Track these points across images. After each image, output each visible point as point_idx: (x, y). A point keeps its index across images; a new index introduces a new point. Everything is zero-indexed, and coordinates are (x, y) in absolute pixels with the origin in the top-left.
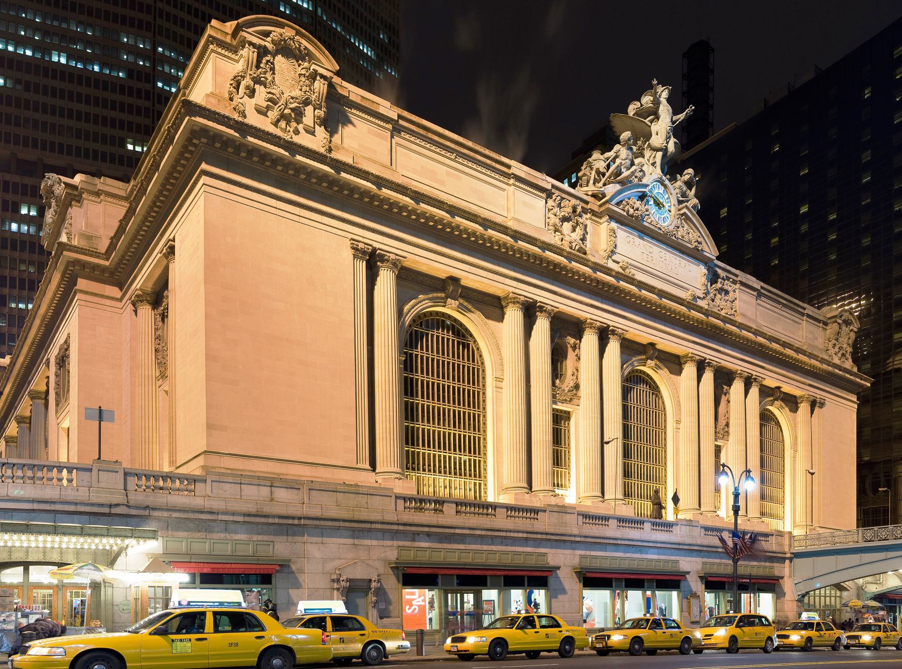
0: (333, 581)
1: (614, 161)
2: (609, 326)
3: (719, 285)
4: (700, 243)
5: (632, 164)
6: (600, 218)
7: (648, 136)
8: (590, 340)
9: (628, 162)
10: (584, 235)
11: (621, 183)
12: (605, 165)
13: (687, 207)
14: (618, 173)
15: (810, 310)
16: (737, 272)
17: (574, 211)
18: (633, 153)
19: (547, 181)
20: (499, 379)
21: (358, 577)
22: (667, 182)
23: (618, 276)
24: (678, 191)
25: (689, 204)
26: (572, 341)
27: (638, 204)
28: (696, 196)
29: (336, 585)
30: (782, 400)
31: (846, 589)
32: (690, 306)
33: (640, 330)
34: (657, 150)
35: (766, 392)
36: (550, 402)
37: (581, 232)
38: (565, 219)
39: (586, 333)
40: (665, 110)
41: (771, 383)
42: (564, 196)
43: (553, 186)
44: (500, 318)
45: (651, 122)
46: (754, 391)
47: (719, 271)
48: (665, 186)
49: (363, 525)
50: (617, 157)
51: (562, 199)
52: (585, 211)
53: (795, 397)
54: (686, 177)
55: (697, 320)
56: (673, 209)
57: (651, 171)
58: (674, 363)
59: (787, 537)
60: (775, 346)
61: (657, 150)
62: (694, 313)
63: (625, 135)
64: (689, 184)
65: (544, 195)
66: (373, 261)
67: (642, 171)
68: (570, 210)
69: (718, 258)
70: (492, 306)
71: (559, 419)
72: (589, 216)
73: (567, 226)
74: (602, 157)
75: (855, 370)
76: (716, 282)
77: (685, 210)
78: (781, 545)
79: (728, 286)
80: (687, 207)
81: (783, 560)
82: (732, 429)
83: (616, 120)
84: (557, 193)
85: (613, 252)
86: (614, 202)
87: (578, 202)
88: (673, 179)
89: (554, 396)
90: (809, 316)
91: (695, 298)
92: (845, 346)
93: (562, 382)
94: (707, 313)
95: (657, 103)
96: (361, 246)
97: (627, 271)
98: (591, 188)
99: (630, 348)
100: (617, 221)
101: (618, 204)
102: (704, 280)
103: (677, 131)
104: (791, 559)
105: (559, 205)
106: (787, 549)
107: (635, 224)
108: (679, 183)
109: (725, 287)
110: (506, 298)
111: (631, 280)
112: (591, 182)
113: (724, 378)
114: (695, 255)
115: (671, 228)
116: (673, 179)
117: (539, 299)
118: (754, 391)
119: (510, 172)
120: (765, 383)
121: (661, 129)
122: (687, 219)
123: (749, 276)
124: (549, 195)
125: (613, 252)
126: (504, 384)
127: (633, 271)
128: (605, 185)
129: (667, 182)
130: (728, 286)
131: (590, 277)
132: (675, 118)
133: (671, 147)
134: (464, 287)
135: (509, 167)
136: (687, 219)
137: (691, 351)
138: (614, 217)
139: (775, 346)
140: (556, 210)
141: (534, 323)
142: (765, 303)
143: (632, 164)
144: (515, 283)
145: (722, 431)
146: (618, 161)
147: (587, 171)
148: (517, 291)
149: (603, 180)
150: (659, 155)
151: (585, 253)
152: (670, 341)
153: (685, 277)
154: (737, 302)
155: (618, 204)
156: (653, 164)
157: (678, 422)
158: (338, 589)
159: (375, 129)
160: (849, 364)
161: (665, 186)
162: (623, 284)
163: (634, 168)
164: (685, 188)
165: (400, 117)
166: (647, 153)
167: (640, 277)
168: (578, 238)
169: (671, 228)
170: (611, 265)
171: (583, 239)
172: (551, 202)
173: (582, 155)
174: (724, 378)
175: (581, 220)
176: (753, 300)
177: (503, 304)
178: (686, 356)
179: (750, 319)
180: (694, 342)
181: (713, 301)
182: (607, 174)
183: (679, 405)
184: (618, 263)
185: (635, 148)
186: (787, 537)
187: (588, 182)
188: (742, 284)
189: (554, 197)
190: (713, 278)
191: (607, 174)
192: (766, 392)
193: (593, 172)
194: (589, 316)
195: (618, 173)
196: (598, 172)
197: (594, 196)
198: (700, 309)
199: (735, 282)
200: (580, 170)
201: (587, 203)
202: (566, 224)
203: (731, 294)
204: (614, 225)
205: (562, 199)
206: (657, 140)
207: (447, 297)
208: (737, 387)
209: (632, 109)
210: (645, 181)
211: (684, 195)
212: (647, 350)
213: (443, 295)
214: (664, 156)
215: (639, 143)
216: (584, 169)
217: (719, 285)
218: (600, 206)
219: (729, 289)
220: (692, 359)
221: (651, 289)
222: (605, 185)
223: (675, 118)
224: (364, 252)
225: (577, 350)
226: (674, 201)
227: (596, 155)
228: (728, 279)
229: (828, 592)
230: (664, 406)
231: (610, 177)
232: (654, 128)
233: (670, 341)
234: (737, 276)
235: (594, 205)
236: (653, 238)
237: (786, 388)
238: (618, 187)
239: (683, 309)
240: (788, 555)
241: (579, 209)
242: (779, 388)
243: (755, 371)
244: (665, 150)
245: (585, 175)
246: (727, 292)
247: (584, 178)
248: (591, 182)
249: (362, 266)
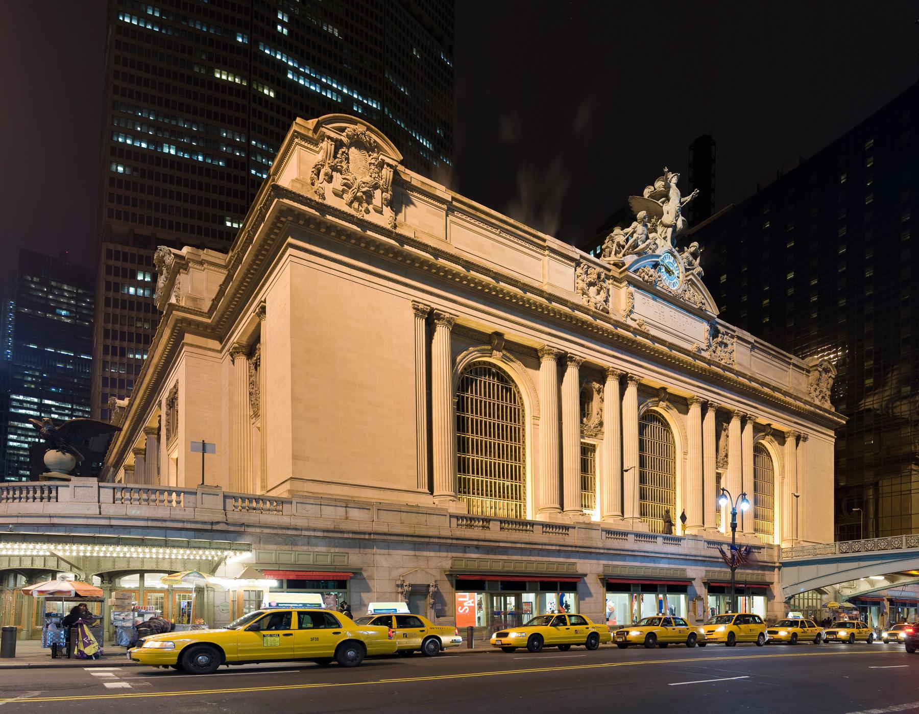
0: (398, 586)
1: (632, 235)
3: (719, 339)
4: (704, 304)
5: (647, 238)
6: (621, 283)
7: (660, 215)
8: (612, 386)
9: (644, 237)
11: (638, 254)
12: (624, 239)
13: (692, 274)
14: (635, 246)
15: (795, 360)
16: (735, 328)
17: (599, 277)
18: (648, 229)
19: (576, 253)
20: (536, 418)
21: (419, 582)
22: (676, 253)
23: (636, 332)
24: (685, 260)
25: (695, 272)
26: (596, 385)
27: (652, 271)
28: (700, 265)
29: (400, 590)
30: (773, 435)
31: (826, 593)
32: (695, 356)
33: (654, 377)
34: (668, 226)
35: (759, 429)
36: (714, 466)
38: (591, 284)
39: (608, 379)
40: (674, 193)
41: (763, 421)
42: (590, 264)
43: (581, 257)
44: (537, 367)
46: (749, 428)
47: (720, 327)
48: (675, 257)
49: (566, 549)
50: (634, 232)
51: (589, 267)
52: (608, 277)
53: (783, 432)
54: (692, 249)
55: (701, 368)
56: (681, 276)
57: (663, 245)
58: (682, 404)
59: (776, 549)
60: (766, 390)
61: (668, 226)
62: (698, 363)
63: (642, 214)
64: (694, 255)
65: (574, 264)
66: (431, 319)
67: (655, 244)
68: (595, 276)
69: (719, 317)
71: (587, 451)
72: (611, 281)
73: (593, 290)
74: (622, 232)
75: (833, 410)
76: (717, 337)
77: (691, 277)
78: (772, 556)
79: (727, 340)
80: (692, 274)
82: (730, 459)
83: (634, 201)
84: (585, 262)
85: (631, 312)
87: (602, 270)
88: (681, 251)
89: (582, 432)
90: (794, 365)
91: (700, 350)
92: (824, 390)
93: (589, 420)
94: (709, 363)
95: (667, 187)
96: (421, 306)
97: (643, 327)
98: (613, 258)
99: (645, 392)
100: (635, 286)
101: (635, 271)
102: (707, 335)
103: (685, 210)
104: (779, 568)
105: (586, 273)
106: (776, 560)
107: (650, 288)
108: (686, 254)
109: (725, 341)
110: (542, 350)
111: (646, 335)
112: (613, 253)
113: (723, 417)
114: (699, 314)
115: (680, 292)
116: (681, 251)
117: (569, 351)
118: (749, 428)
119: (545, 244)
120: (758, 421)
122: (693, 284)
123: (744, 332)
124: (578, 264)
125: (631, 312)
126: (540, 422)
127: (648, 328)
128: (624, 255)
129: (676, 253)
130: (727, 340)
131: (612, 332)
132: (683, 200)
133: (680, 224)
135: (544, 240)
136: (693, 284)
137: (696, 394)
138: (631, 282)
139: (766, 390)
140: (584, 276)
141: (565, 371)
142: (757, 354)
143: (647, 238)
144: (549, 338)
145: (722, 460)
146: (635, 236)
147: (609, 244)
148: (551, 344)
149: (623, 251)
150: (670, 230)
151: (608, 313)
152: (679, 386)
153: (692, 333)
154: (734, 353)
156: (665, 238)
157: (685, 453)
158: (402, 593)
159: (432, 209)
160: (828, 405)
161: (675, 257)
162: (639, 338)
163: (648, 241)
164: (691, 258)
165: (453, 198)
166: (660, 229)
167: (653, 332)
168: (602, 300)
170: (629, 322)
171: (606, 301)
172: (579, 270)
173: (604, 231)
174: (723, 417)
175: (604, 285)
176: (748, 352)
177: (540, 355)
178: (692, 398)
179: (745, 368)
180: (795, 423)
182: (626, 247)
183: (686, 439)
185: (649, 225)
187: (610, 253)
188: (739, 338)
190: (715, 333)
191: (626, 247)
192: (759, 429)
193: (615, 245)
194: (611, 365)
195: (635, 246)
196: (619, 245)
197: (615, 264)
198: (703, 359)
199: (732, 337)
200: (604, 243)
201: (609, 270)
202: (592, 288)
203: (730, 346)
204: (632, 289)
205: (589, 267)
206: (668, 218)
207: (492, 349)
208: (735, 423)
209: (647, 192)
210: (657, 252)
211: (690, 264)
212: (660, 393)
213: (490, 347)
214: (674, 231)
215: (653, 220)
216: (608, 242)
217: (719, 339)
218: (621, 273)
219: (728, 342)
220: (697, 401)
221: (663, 342)
222: (624, 255)
223: (683, 200)
224: (423, 312)
226: (682, 269)
227: (617, 230)
228: (727, 334)
231: (628, 249)
232: (665, 208)
233: (679, 386)
234: (734, 331)
235: (615, 272)
236: (664, 300)
237: (776, 425)
238: (635, 257)
239: (690, 359)
240: (777, 565)
241: (603, 276)
242: (769, 425)
243: (749, 411)
244: (674, 227)
245: (607, 247)
246: (726, 345)
247: (607, 250)
248: (613, 253)
249: (422, 323)
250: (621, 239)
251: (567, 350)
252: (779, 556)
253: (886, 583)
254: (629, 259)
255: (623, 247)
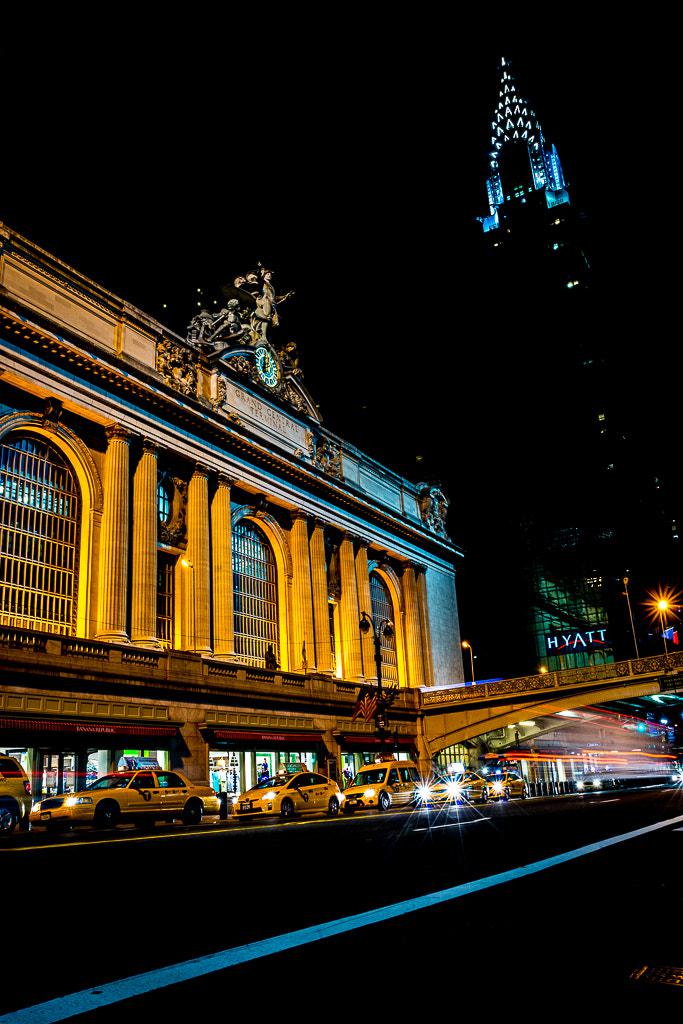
1: (221, 322)
2: (218, 471)
7: (254, 306)
10: (194, 382)
13: (292, 375)
17: (185, 355)
25: (295, 372)
33: (252, 480)
37: (191, 379)
38: (174, 364)
45: (256, 295)
52: (195, 360)
57: (256, 334)
59: (416, 694)
67: (248, 335)
70: (94, 436)
72: (199, 365)
73: (177, 372)
78: (413, 703)
80: (292, 375)
81: (413, 719)
86: (224, 357)
101: (228, 360)
104: (422, 717)
106: (417, 707)
110: (111, 429)
114: (301, 417)
121: (264, 304)
122: (292, 384)
127: (243, 424)
133: (276, 321)
134: (65, 411)
135: (121, 306)
138: (223, 370)
140: (167, 354)
144: (122, 416)
145: (334, 586)
146: (226, 323)
148: (123, 423)
150: (265, 325)
155: (228, 360)
157: (290, 576)
160: (443, 535)
166: (253, 323)
169: (278, 390)
171: (194, 385)
172: (161, 346)
176: (355, 468)
181: (319, 461)
183: (291, 560)
184: (228, 413)
186: (416, 694)
189: (165, 342)
190: (320, 442)
204: (223, 378)
207: (45, 418)
211: (288, 363)
212: (256, 501)
213: (41, 416)
222: (213, 340)
225: (184, 492)
228: (332, 444)
229: (457, 750)
230: (275, 559)
231: (218, 334)
240: (420, 713)
241: (190, 358)
244: (270, 322)
245: (194, 328)
250: (210, 324)
251: (143, 433)
252: (420, 703)
253: (538, 730)
254: (220, 346)
255: (213, 333)
